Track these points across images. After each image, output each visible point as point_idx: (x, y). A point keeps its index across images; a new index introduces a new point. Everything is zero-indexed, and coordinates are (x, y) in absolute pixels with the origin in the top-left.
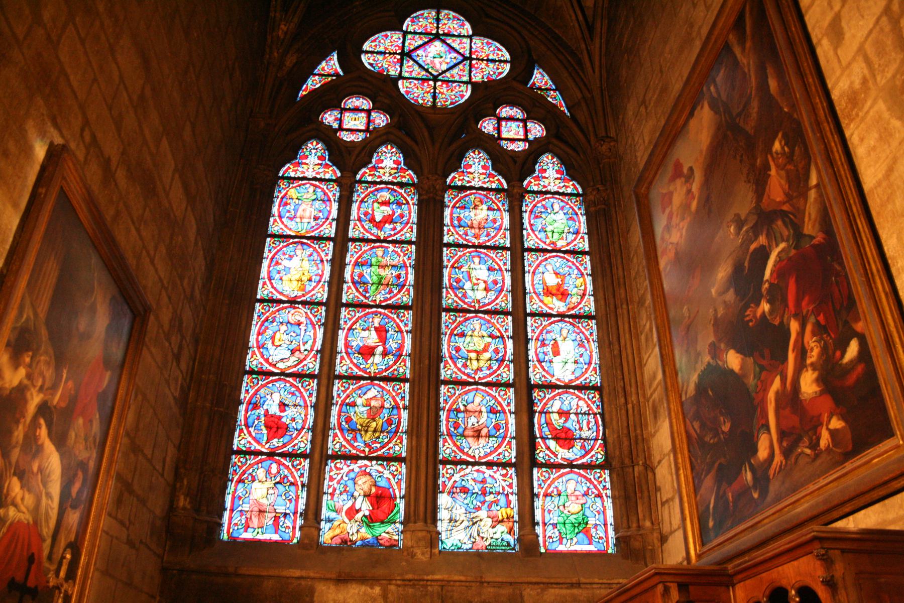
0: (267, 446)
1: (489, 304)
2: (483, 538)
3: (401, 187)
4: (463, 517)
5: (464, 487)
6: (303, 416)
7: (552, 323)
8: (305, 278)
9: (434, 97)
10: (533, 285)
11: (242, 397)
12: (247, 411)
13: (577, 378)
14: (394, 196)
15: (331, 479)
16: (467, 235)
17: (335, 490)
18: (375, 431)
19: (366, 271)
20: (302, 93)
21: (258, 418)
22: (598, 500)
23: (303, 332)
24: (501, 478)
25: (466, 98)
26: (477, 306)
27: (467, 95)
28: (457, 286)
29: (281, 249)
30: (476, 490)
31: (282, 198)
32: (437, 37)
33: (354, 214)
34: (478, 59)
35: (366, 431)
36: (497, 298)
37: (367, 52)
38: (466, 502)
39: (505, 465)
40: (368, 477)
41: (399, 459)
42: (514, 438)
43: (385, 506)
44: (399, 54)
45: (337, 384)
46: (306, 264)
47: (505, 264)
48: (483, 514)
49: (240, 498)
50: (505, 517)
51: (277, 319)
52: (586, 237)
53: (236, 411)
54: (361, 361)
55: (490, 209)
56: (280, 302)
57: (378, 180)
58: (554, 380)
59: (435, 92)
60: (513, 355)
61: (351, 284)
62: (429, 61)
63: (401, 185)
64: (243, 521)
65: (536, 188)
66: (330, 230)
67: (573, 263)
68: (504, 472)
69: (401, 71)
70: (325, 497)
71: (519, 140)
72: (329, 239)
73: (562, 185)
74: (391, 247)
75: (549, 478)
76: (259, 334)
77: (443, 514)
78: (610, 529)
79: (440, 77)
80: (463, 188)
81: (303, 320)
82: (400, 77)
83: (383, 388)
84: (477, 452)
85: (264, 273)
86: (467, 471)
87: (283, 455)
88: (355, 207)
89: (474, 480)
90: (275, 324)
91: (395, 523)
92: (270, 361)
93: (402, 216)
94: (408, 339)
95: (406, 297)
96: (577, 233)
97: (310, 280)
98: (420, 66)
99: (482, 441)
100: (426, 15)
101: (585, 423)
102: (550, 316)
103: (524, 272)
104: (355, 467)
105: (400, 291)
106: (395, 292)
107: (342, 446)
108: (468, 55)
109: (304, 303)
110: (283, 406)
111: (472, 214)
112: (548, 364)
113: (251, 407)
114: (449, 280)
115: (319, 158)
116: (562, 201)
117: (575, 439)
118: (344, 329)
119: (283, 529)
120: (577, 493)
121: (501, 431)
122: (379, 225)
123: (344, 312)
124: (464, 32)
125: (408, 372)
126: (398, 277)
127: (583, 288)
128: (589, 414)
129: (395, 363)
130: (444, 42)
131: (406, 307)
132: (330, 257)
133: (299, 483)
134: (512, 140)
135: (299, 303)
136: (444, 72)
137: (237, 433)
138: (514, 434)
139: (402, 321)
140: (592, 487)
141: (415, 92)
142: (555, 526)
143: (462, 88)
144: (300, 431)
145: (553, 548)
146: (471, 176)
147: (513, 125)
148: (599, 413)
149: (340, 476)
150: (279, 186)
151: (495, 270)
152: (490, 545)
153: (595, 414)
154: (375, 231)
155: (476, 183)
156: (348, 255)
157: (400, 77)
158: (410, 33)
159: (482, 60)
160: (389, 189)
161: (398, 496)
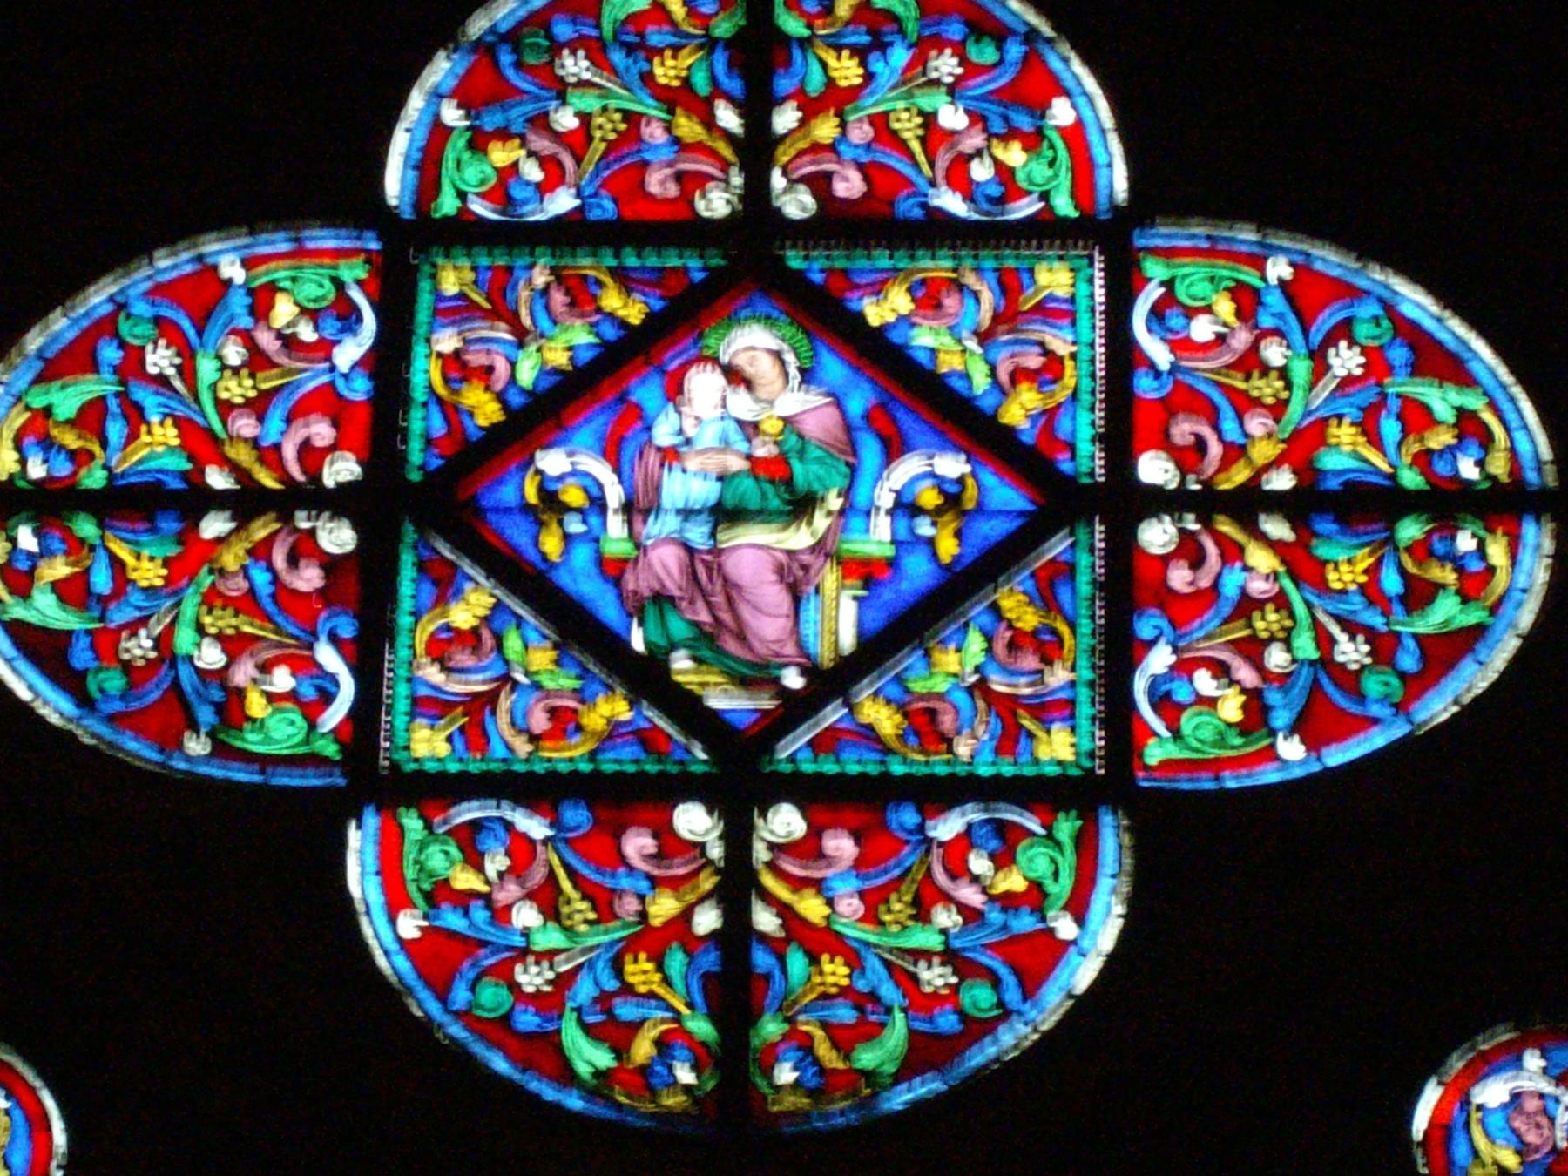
9: (734, 987)
25: (1082, 973)
27: (1094, 939)
32: (750, 264)
34: (1207, 503)
44: (339, 502)
59: (737, 932)
62: (666, 563)
82: (366, 775)
98: (575, 629)
108: (1087, 458)
130: (825, 317)
136: (834, 680)
143: (1035, 861)
158: (464, 233)
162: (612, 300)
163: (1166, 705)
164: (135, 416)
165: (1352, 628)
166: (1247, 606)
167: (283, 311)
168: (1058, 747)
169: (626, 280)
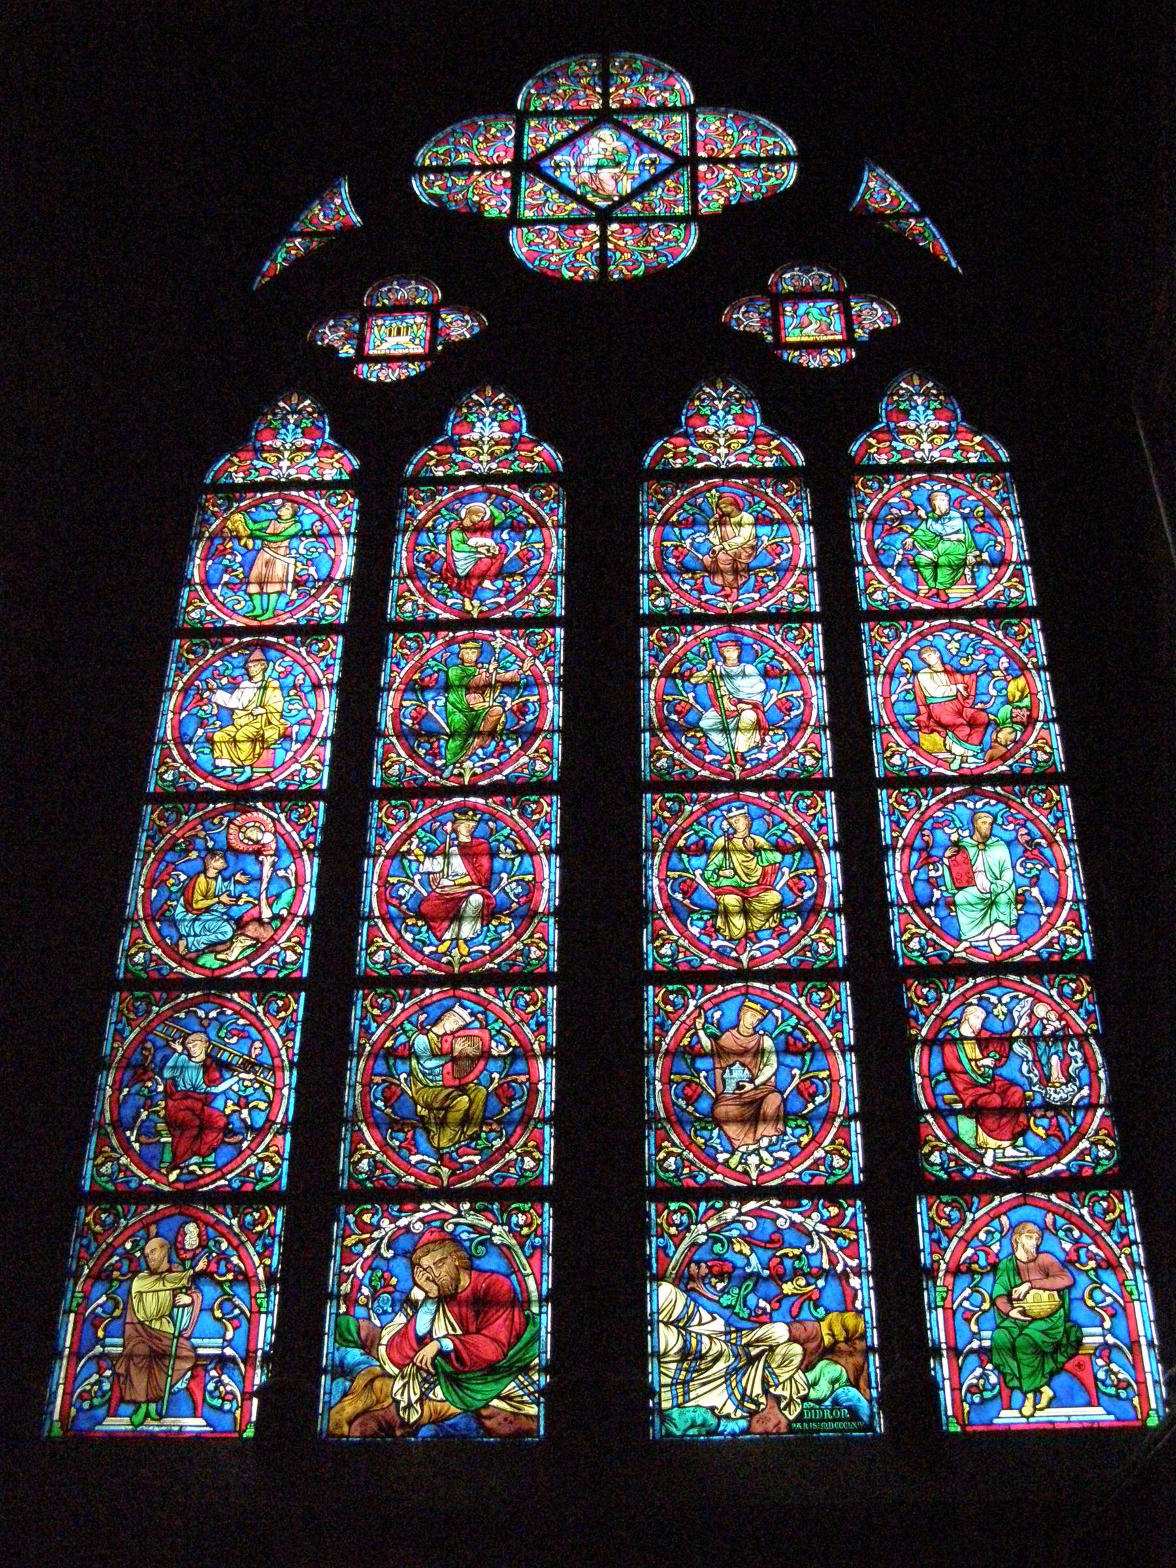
0: (173, 1176)
1: (770, 763)
2: (778, 1399)
3: (523, 488)
4: (716, 1349)
5: (720, 1258)
6: (269, 1090)
7: (945, 801)
8: (271, 734)
9: (603, 260)
10: (889, 706)
11: (107, 1049)
12: (117, 1087)
13: (1026, 943)
14: (504, 510)
15: (348, 1256)
16: (703, 591)
17: (357, 1286)
18: (466, 1119)
19: (435, 704)
20: (259, 281)
21: (149, 1101)
22: (1108, 1276)
23: (267, 872)
24: (823, 1228)
25: (686, 254)
26: (737, 770)
28: (680, 726)
29: (210, 663)
30: (755, 1265)
31: (211, 538)
32: (604, 117)
33: (402, 560)
35: (442, 1123)
36: (790, 747)
37: (425, 170)
38: (726, 1300)
39: (834, 1193)
40: (449, 1247)
41: (532, 1193)
42: (855, 1117)
43: (500, 1326)
45: (361, 1003)
46: (274, 698)
47: (809, 656)
48: (778, 1331)
49: (96, 1321)
50: (841, 1336)
51: (199, 843)
52: (1027, 571)
53: (92, 1089)
54: (423, 936)
55: (759, 521)
56: (210, 796)
57: (462, 473)
58: (960, 952)
59: (603, 249)
60: (845, 892)
61: (394, 739)
62: (585, 176)
63: (524, 480)
64: (106, 1386)
65: (883, 460)
66: (335, 607)
67: (996, 641)
68: (834, 1211)
69: (515, 207)
70: (330, 1308)
71: (832, 345)
72: (333, 629)
73: (953, 445)
74: (499, 638)
75: (963, 1220)
76: (152, 883)
77: (668, 1339)
78: (1150, 1362)
79: (618, 213)
80: (688, 476)
81: (268, 838)
83: (485, 1004)
84: (753, 1160)
85: (166, 728)
86: (730, 1214)
87: (218, 1199)
88: (402, 543)
89: (748, 1238)
90: (194, 855)
91: (526, 1370)
92: (182, 949)
93: (524, 558)
94: (551, 871)
95: (544, 759)
96: (1001, 562)
97: (286, 737)
98: (564, 191)
99: (767, 1131)
100: (574, 67)
101: (1055, 1060)
102: (941, 781)
103: (862, 675)
104: (413, 1221)
105: (524, 748)
106: (514, 749)
107: (376, 1165)
108: (685, 151)
109: (272, 796)
110: (215, 1067)
111: (714, 538)
112: (943, 912)
113: (128, 1075)
114: (659, 710)
115: (305, 434)
116: (956, 485)
117: (1029, 1110)
118: (376, 856)
119: (217, 1402)
120: (1044, 1259)
121: (819, 1099)
122: (467, 585)
123: (378, 812)
124: (673, 100)
125: (553, 956)
126: (522, 710)
127: (1026, 702)
128: (1066, 1039)
129: (517, 935)
130: (622, 127)
131: (543, 787)
132: (336, 676)
133: (260, 1272)
134: (813, 347)
135: (257, 796)
136: (626, 199)
137: (92, 1147)
138: (855, 1106)
139: (533, 824)
140: (1086, 1239)
141: (551, 250)
142: (984, 1354)
143: (676, 232)
144: (260, 1132)
145: (985, 1419)
146: (708, 443)
147: (814, 311)
148: (1095, 1034)
149: (368, 1252)
150: (204, 509)
151: (781, 673)
152: (800, 1418)
153: (1083, 1038)
154: (454, 600)
155: (724, 457)
156: (387, 665)
157: (514, 220)
158: (536, 114)
159: (725, 161)
160: (490, 492)
161: (534, 1295)
162: (571, 126)
163: (705, 200)
164: (458, 152)
165: (750, 185)
166: (724, 181)
167: (493, 130)
168: (680, 210)
169: (575, 122)
